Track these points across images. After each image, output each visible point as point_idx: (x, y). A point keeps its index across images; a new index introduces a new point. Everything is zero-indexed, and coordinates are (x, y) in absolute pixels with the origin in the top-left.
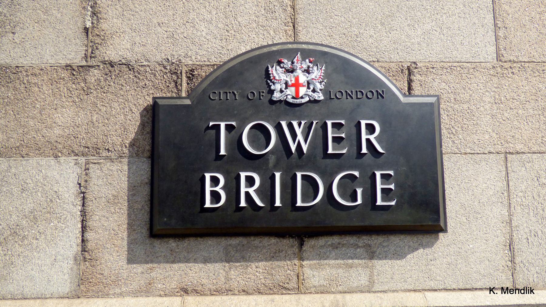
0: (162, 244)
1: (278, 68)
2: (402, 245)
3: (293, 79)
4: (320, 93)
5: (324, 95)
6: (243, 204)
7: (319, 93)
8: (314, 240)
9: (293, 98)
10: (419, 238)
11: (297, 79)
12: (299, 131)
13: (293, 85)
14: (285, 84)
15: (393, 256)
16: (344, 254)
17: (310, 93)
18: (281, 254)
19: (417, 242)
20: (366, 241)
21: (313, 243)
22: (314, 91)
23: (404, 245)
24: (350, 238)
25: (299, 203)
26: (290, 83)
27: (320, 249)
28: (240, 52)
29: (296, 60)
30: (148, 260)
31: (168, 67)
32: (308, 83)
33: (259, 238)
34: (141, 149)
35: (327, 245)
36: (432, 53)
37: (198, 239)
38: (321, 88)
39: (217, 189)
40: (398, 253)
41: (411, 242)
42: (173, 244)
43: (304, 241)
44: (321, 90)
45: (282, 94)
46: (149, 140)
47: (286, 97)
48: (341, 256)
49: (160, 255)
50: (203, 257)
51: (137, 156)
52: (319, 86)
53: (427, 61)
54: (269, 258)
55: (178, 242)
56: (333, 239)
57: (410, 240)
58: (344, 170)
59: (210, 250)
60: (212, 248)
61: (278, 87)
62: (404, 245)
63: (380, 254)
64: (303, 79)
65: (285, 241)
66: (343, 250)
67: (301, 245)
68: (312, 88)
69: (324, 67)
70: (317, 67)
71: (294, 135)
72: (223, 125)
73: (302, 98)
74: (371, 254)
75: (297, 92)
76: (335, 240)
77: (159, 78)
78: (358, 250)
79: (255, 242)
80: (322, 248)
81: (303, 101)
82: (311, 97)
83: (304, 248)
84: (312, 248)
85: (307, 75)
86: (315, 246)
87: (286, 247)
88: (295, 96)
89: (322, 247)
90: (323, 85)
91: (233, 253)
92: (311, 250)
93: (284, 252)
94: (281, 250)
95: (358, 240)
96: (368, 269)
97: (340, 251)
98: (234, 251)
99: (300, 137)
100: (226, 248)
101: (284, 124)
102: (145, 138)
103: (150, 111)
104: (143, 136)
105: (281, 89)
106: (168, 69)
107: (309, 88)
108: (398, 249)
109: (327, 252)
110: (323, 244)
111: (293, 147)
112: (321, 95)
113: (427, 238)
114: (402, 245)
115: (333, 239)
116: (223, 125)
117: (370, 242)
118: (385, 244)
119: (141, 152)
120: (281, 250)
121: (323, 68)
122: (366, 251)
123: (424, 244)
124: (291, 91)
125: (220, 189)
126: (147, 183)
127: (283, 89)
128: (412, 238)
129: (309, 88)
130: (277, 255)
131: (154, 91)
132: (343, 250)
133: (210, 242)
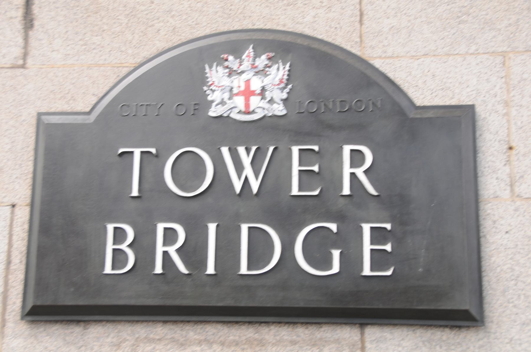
1: (220, 69)
7: (279, 104)
11: (248, 82)
12: (246, 160)
22: (271, 101)
26: (235, 91)
61: (215, 96)
64: (256, 84)
71: (239, 167)
72: (137, 152)
73: (253, 112)
111: (238, 185)
116: (137, 152)
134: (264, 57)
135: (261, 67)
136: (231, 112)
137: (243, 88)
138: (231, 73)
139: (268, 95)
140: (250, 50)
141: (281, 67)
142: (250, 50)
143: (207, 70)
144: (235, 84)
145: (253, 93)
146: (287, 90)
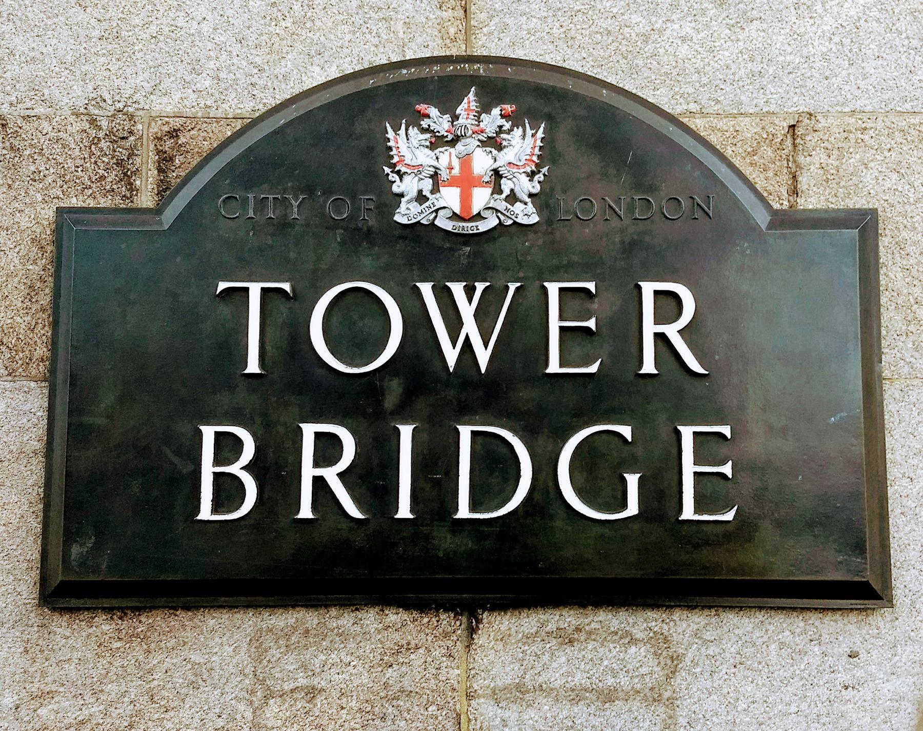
0: (75, 626)
1: (413, 131)
2: (760, 640)
3: (456, 163)
4: (530, 205)
5: (540, 210)
6: (306, 512)
8: (507, 617)
9: (455, 217)
10: (811, 622)
11: (466, 161)
12: (467, 311)
13: (452, 182)
14: (432, 177)
15: (734, 670)
16: (592, 660)
17: (502, 205)
18: (413, 656)
19: (805, 632)
20: (654, 624)
21: (503, 628)
22: (512, 198)
23: (765, 638)
24: (610, 616)
25: (464, 512)
26: (444, 175)
27: (524, 644)
28: (309, 84)
29: (465, 110)
30: (32, 670)
31: (104, 124)
32: (497, 174)
33: (352, 611)
34: (21, 355)
35: (543, 634)
36: (862, 84)
37: (178, 613)
38: (534, 191)
39: (234, 469)
40: (749, 663)
41: (787, 633)
42: (106, 627)
43: (479, 621)
44: (531, 195)
45: (424, 206)
46: (46, 328)
47: (434, 214)
48: (582, 667)
49: (68, 657)
50: (189, 666)
51: (10, 374)
52: (526, 186)
53: (847, 109)
54: (380, 669)
55: (120, 622)
56: (561, 615)
57: (785, 625)
58: (597, 422)
59: (211, 643)
60: (217, 639)
61: (408, 186)
62: (766, 637)
63: (695, 664)
65: (426, 620)
66: (590, 648)
67: (472, 631)
68: (507, 192)
69: (541, 130)
70: (524, 131)
71: (454, 323)
72: (255, 290)
73: (479, 217)
74: (669, 662)
75: (466, 200)
76: (568, 620)
77: (77, 152)
78: (633, 649)
79: (340, 622)
80: (530, 641)
81: (483, 227)
82: (502, 213)
83: (481, 639)
84: (502, 640)
85: (495, 152)
86: (510, 635)
87: (430, 638)
88: (457, 211)
89: (529, 638)
90: (539, 182)
91: (275, 653)
92: (500, 646)
93: (421, 651)
94: (413, 645)
95: (631, 621)
96: (661, 709)
97: (580, 650)
98: (279, 648)
99: (470, 328)
100: (256, 639)
101: (426, 289)
102: (33, 324)
103: (49, 248)
104: (29, 318)
105: (420, 192)
106: (104, 128)
107: (498, 190)
108: (749, 651)
109: (543, 654)
110: (533, 631)
111: (451, 355)
112: (530, 208)
113: (836, 621)
114: (760, 640)
115: (561, 615)
116: (255, 290)
117: (665, 627)
118: (708, 636)
119: (20, 362)
120: (413, 645)
121: (540, 134)
122: (655, 654)
123: (825, 637)
124: (450, 198)
125: (243, 471)
126: (35, 453)
127: (426, 193)
128: (788, 621)
129: (498, 190)
130: (402, 660)
131: (63, 191)
132: (590, 648)
133: (212, 622)
134: (496, 111)
135: (490, 130)
136: (436, 217)
137: (456, 171)
138: (437, 142)
139: (506, 186)
140: (470, 101)
141: (529, 132)
142: (470, 101)
143: (391, 134)
144: (443, 163)
145: (478, 182)
146: (540, 177)
